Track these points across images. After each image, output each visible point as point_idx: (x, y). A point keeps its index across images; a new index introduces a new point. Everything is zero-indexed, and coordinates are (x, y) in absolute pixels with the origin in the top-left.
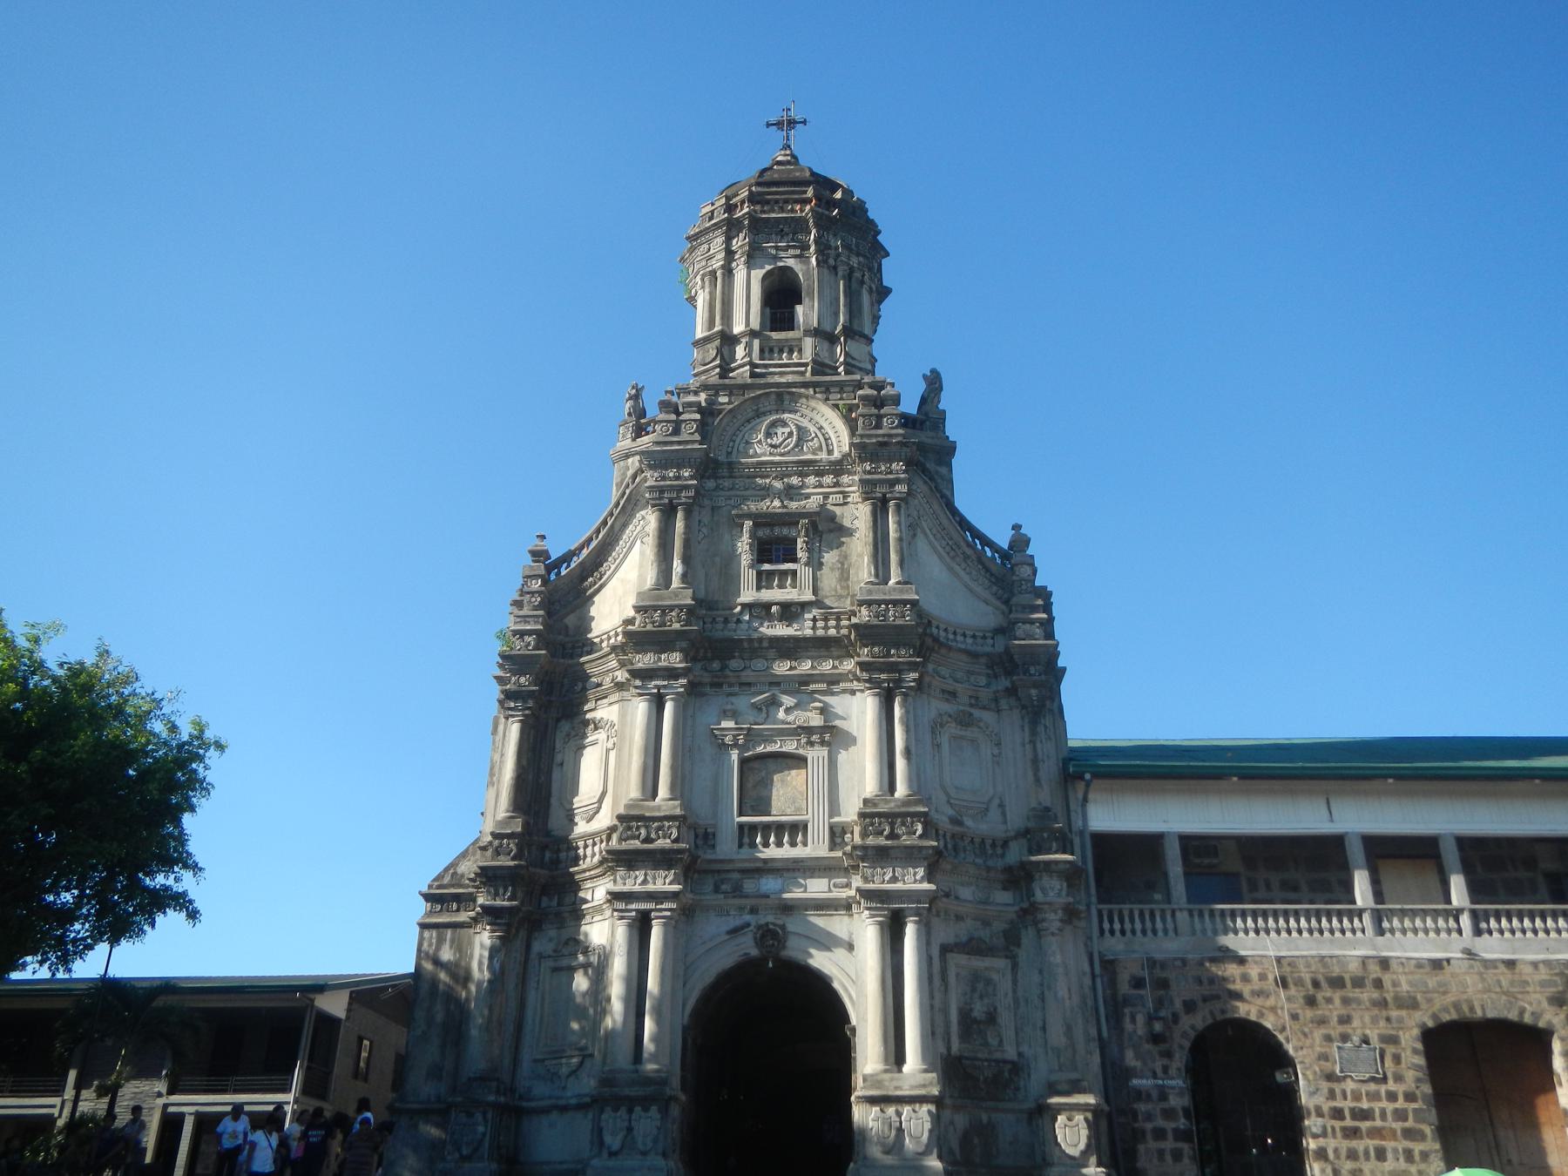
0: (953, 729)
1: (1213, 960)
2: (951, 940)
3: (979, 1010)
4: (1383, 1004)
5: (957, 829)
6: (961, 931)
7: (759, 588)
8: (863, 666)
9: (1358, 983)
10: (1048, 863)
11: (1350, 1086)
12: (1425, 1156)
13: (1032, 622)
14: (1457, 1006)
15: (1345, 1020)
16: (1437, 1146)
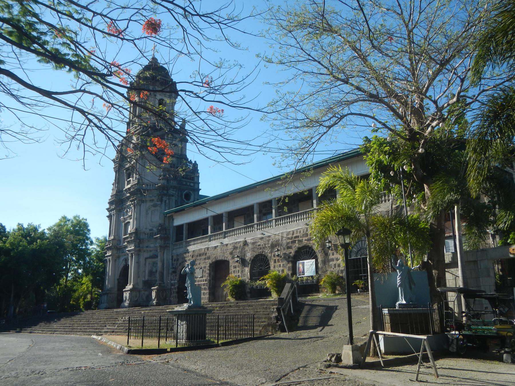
0: (153, 208)
1: (185, 253)
2: (148, 256)
3: (154, 270)
4: (205, 259)
5: (151, 232)
6: (151, 254)
7: (127, 185)
8: (131, 201)
9: (203, 254)
10: (157, 237)
11: (198, 279)
12: (206, 293)
13: (160, 179)
14: (215, 257)
15: (200, 264)
16: (208, 291)
